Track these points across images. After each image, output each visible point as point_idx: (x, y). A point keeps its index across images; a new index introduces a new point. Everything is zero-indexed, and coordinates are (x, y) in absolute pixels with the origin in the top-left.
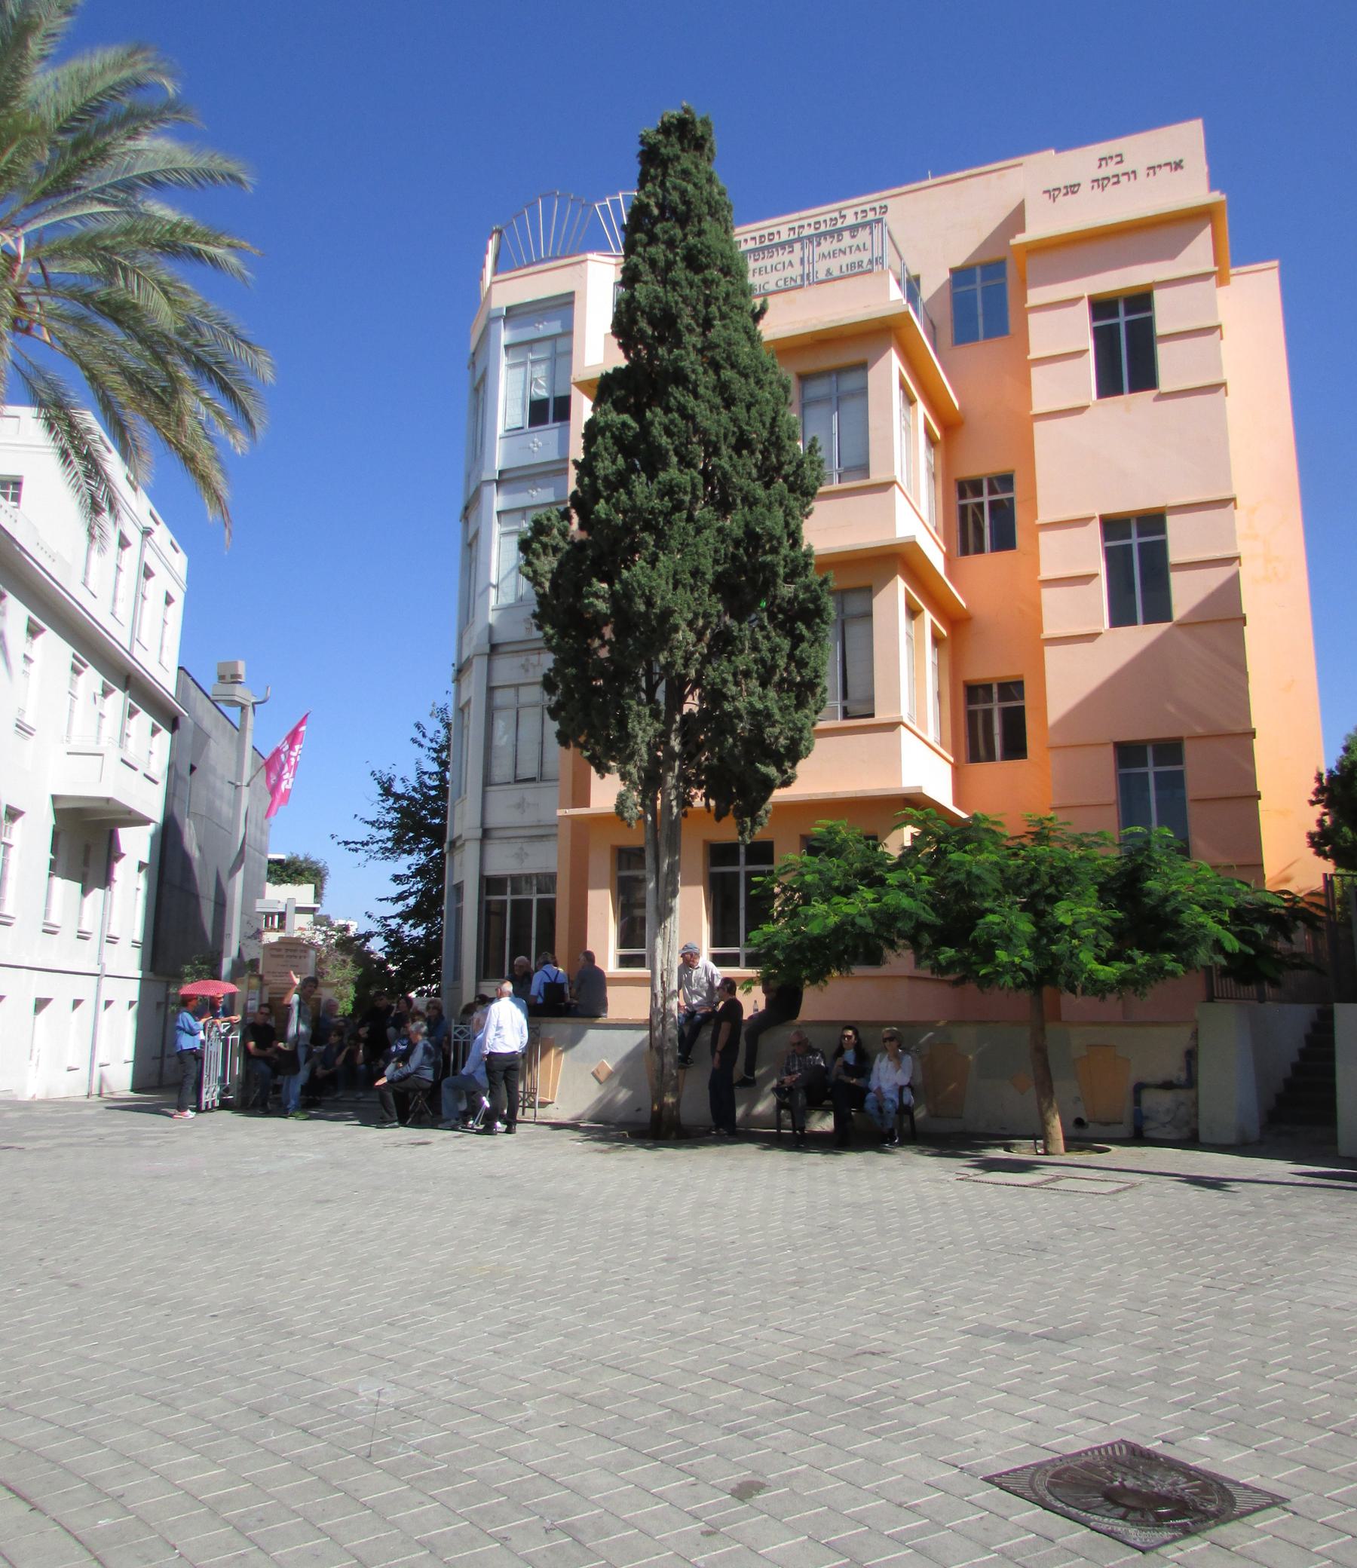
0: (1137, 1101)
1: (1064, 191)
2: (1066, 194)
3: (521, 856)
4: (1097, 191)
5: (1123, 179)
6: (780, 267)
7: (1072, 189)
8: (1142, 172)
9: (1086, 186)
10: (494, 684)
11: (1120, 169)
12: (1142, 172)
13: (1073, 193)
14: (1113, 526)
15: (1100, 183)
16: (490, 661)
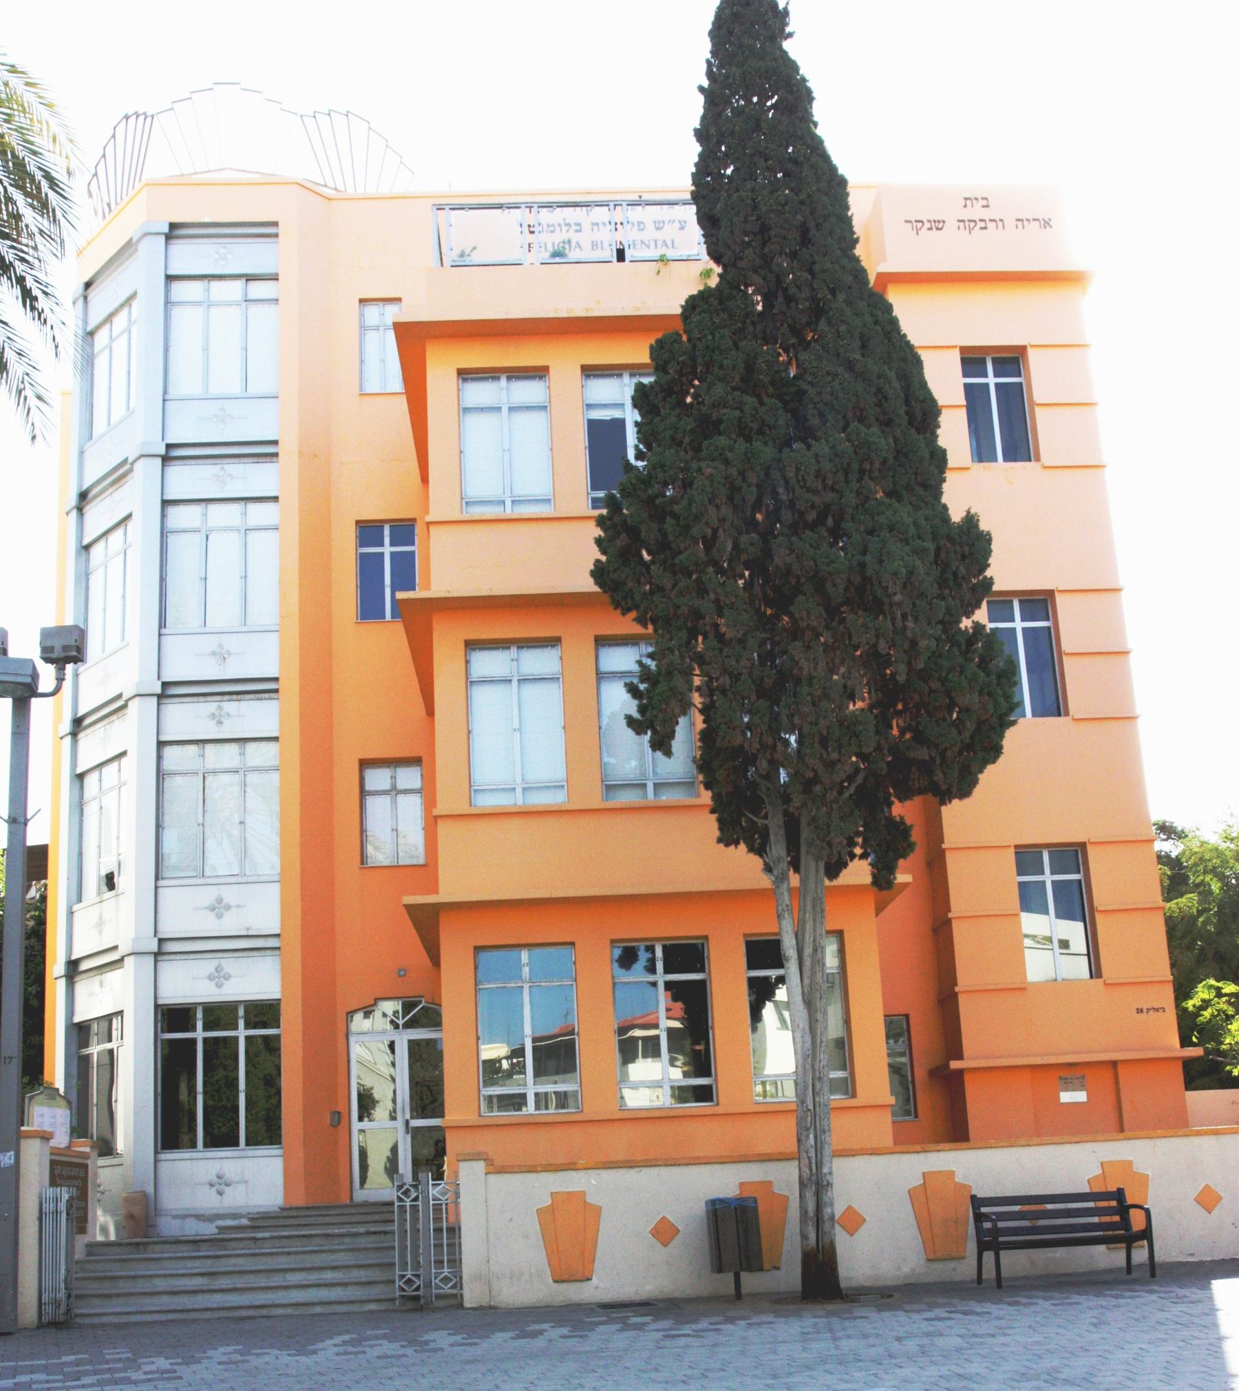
1: (927, 225)
2: (930, 229)
3: (219, 977)
5: (991, 225)
7: (938, 225)
8: (1011, 223)
9: (951, 224)
12: (1011, 223)
13: (938, 229)
15: (968, 224)
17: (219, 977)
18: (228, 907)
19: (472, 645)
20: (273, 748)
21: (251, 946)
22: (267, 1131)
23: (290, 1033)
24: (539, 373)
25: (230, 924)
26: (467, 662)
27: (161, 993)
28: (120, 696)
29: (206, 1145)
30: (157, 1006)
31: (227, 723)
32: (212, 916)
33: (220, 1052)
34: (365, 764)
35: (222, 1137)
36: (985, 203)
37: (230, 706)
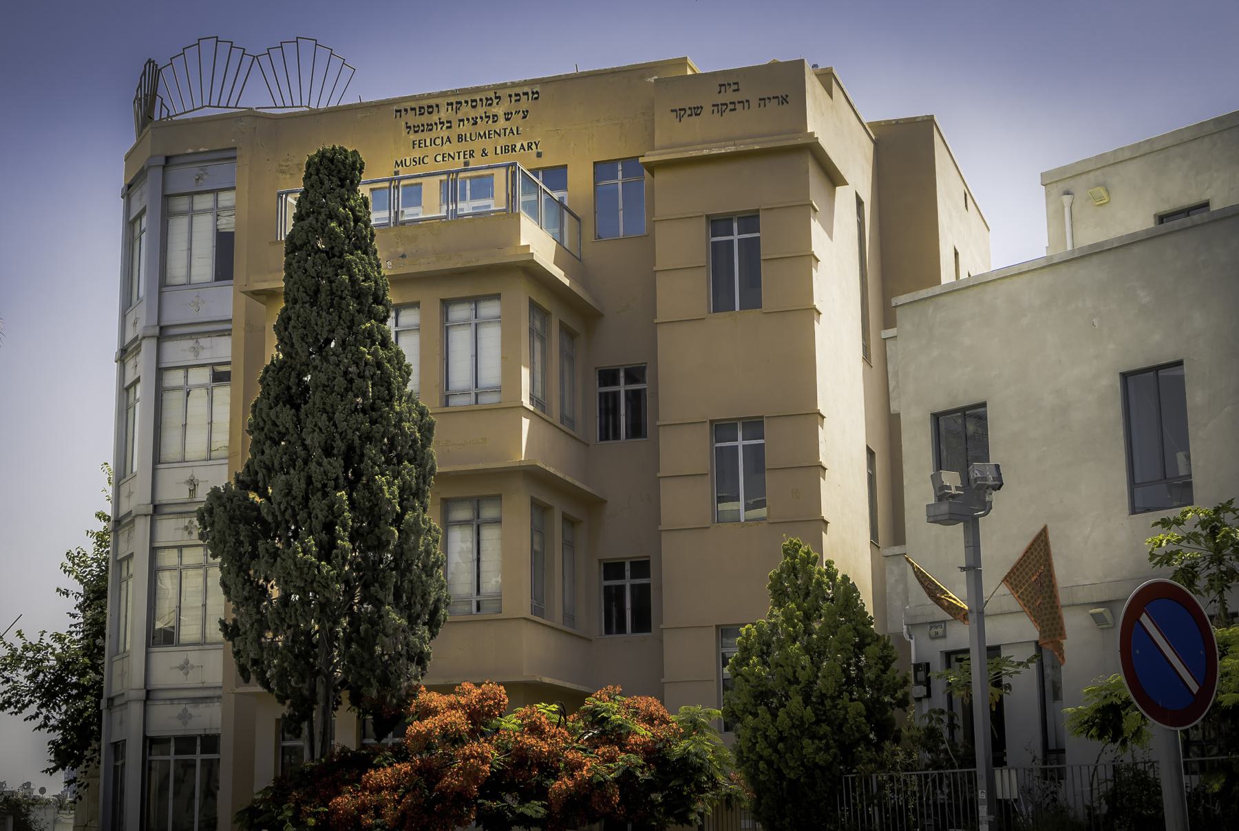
1: (689, 112)
4: (717, 115)
5: (739, 107)
6: (438, 141)
7: (696, 111)
9: (708, 108)
10: (157, 545)
14: (722, 429)
15: (720, 108)
16: (152, 521)
18: (193, 667)
25: (192, 680)
30: (145, 737)
36: (735, 87)
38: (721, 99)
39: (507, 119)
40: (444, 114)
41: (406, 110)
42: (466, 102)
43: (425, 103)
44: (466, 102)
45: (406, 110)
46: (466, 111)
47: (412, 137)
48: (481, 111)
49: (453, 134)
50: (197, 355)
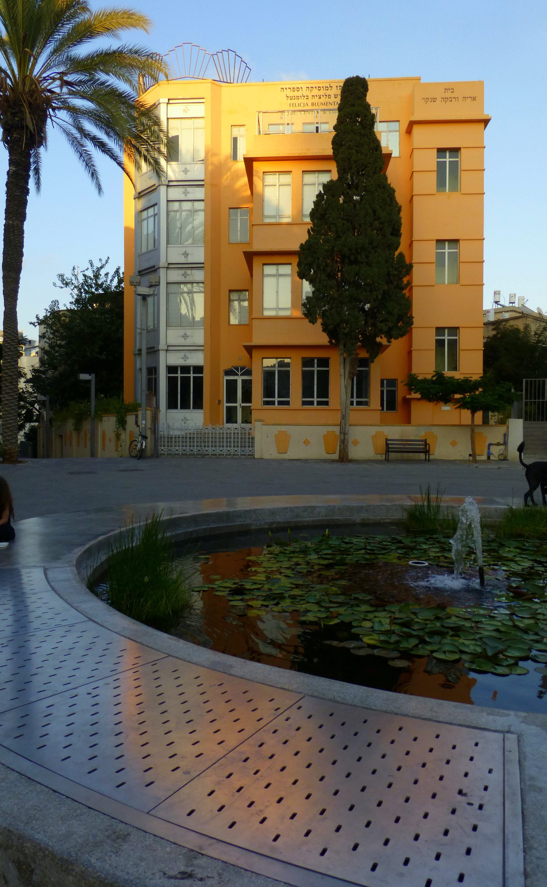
0: (489, 449)
1: (430, 100)
2: (431, 102)
3: (185, 358)
5: (454, 100)
6: (302, 105)
7: (434, 100)
9: (439, 100)
11: (452, 95)
12: (461, 99)
15: (445, 99)
17: (185, 358)
19: (264, 264)
20: (202, 203)
21: (195, 349)
22: (198, 405)
23: (206, 376)
24: (289, 172)
25: (189, 342)
26: (263, 270)
27: (168, 363)
28: (154, 266)
29: (181, 408)
30: (167, 366)
31: (187, 277)
32: (183, 339)
33: (185, 381)
34: (230, 291)
35: (185, 406)
36: (452, 91)
37: (189, 272)
38: (445, 95)
39: (336, 98)
40: (305, 92)
41: (286, 88)
42: (316, 87)
43: (295, 86)
44: (316, 87)
45: (286, 88)
46: (315, 92)
47: (289, 101)
48: (322, 92)
49: (310, 101)
50: (186, 195)
